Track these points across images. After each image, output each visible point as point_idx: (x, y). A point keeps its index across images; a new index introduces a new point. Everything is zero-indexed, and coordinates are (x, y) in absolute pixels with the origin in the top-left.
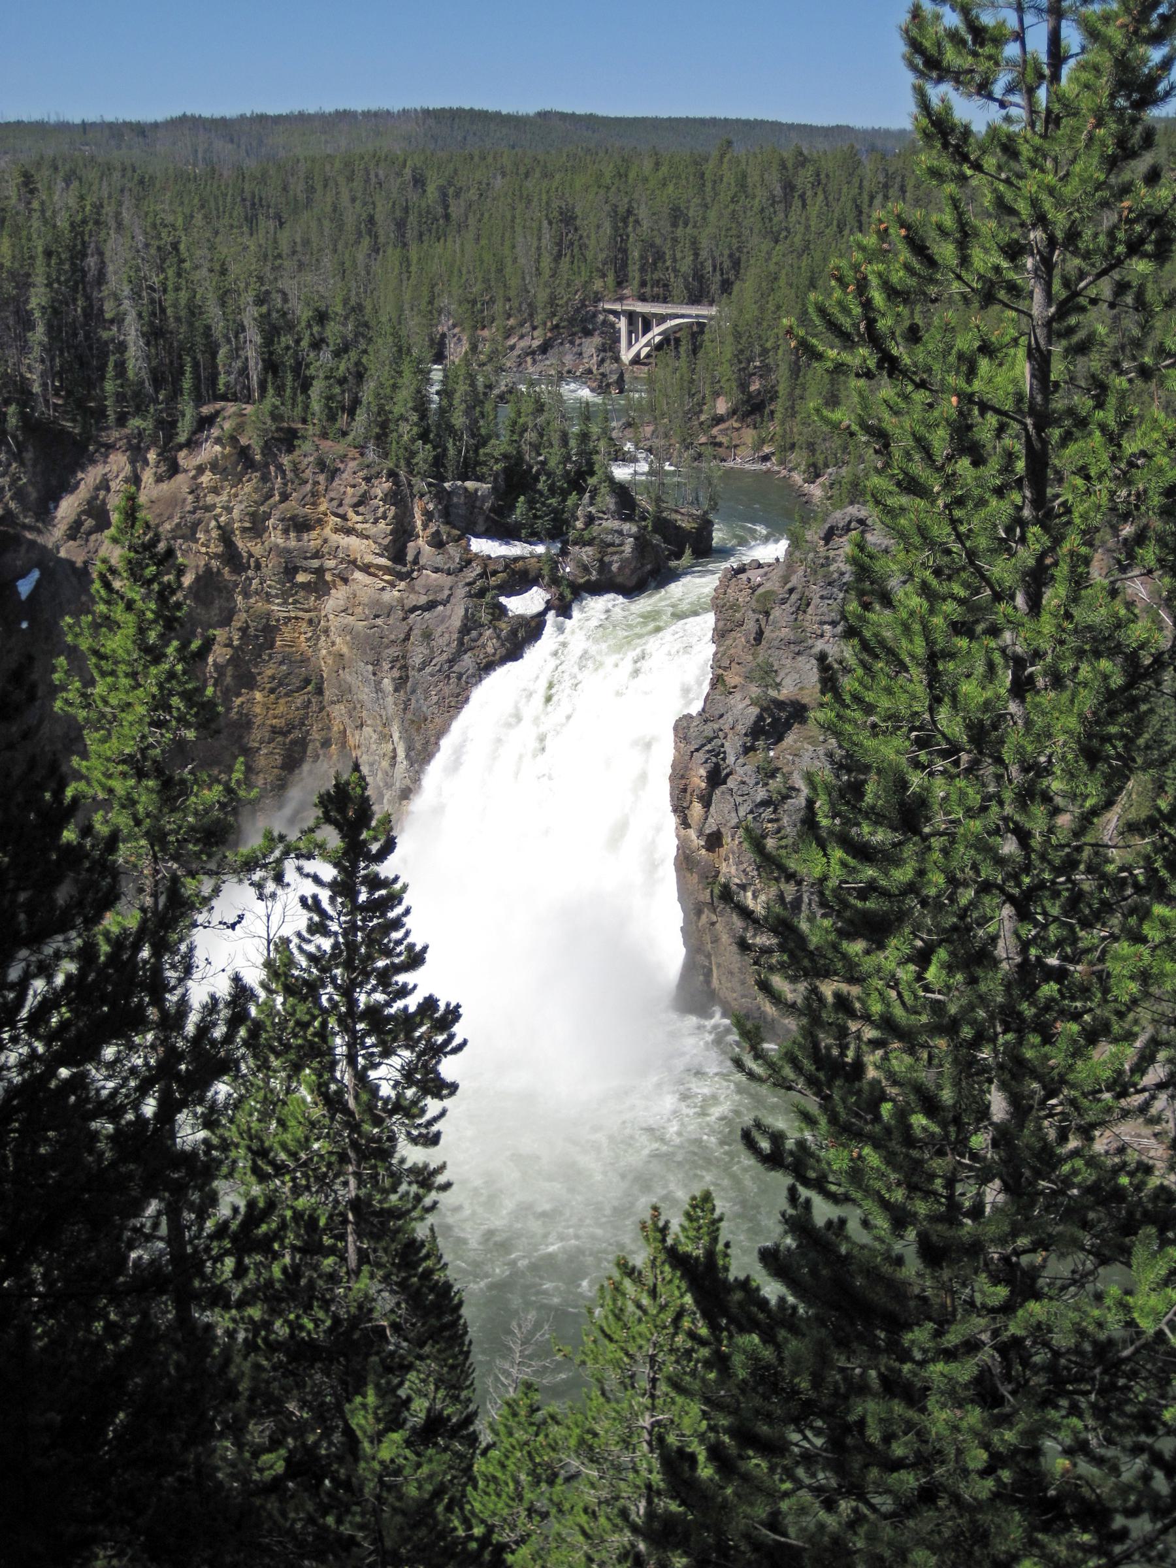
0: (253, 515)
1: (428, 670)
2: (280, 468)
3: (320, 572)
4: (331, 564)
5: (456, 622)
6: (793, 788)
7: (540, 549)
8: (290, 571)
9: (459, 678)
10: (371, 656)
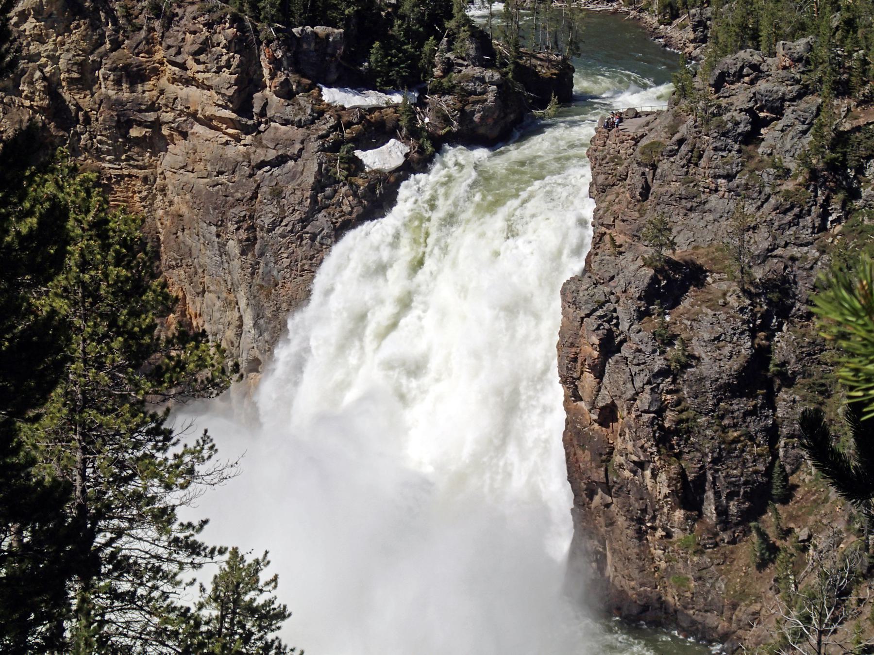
0: (81, 65)
1: (279, 230)
2: (110, 13)
3: (156, 125)
4: (168, 116)
5: (311, 180)
6: (692, 357)
7: (397, 98)
8: (123, 124)
9: (313, 238)
10: (214, 216)
